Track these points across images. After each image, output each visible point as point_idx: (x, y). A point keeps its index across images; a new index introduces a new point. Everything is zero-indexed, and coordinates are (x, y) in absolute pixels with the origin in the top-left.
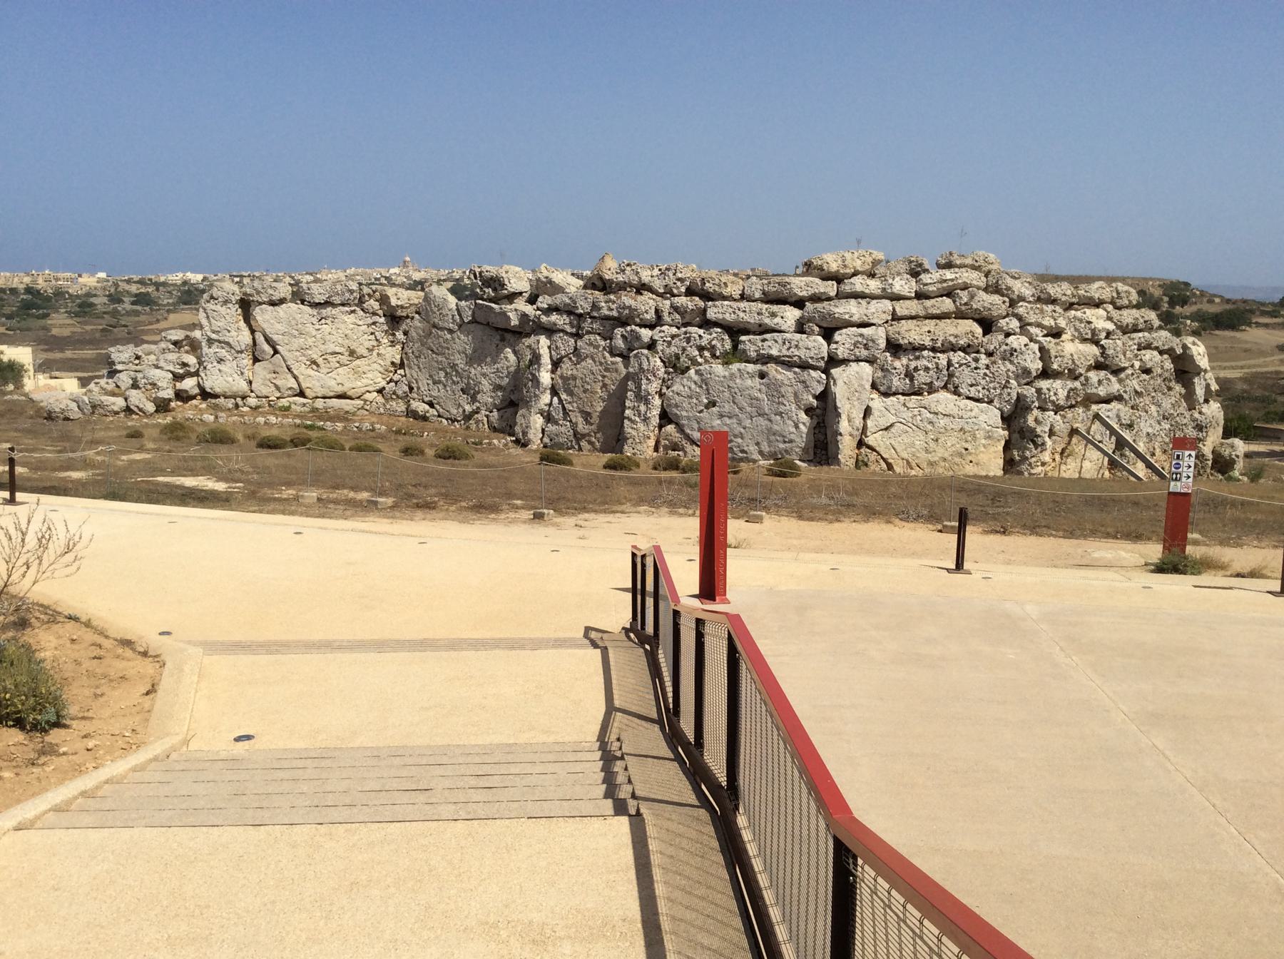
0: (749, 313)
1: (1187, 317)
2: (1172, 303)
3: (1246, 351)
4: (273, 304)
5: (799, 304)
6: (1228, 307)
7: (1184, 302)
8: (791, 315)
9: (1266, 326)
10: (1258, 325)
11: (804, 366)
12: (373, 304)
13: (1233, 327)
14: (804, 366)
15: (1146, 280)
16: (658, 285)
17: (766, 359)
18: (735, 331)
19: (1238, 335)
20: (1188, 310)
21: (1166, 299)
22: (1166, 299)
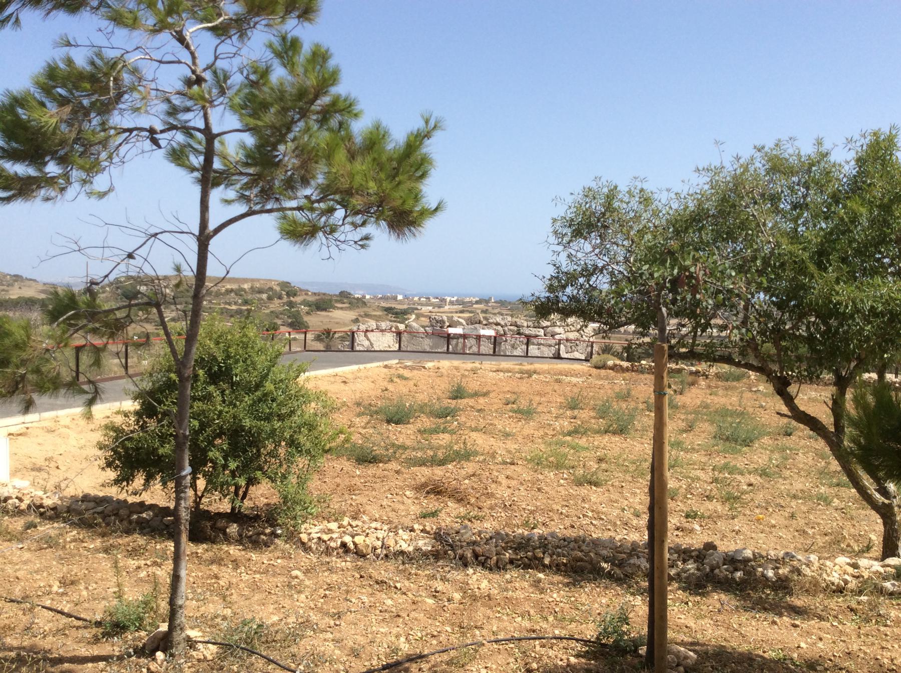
0: (533, 331)
1: (300, 304)
2: (288, 295)
3: (337, 323)
4: (372, 331)
5: (543, 328)
6: (318, 298)
7: (295, 295)
8: (542, 332)
9: (342, 308)
10: (338, 308)
11: (550, 346)
12: (393, 329)
13: (325, 310)
14: (550, 346)
15: (271, 281)
16: (502, 323)
17: (539, 344)
18: (528, 337)
19: (329, 314)
20: (298, 299)
21: (284, 293)
22: (284, 293)
